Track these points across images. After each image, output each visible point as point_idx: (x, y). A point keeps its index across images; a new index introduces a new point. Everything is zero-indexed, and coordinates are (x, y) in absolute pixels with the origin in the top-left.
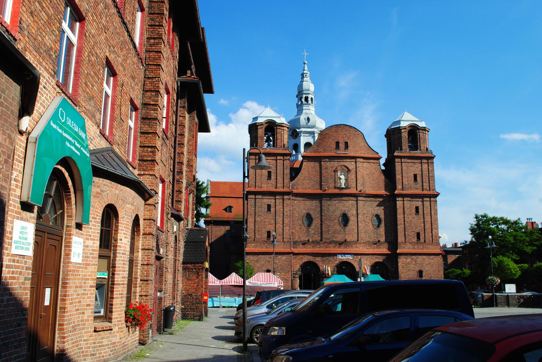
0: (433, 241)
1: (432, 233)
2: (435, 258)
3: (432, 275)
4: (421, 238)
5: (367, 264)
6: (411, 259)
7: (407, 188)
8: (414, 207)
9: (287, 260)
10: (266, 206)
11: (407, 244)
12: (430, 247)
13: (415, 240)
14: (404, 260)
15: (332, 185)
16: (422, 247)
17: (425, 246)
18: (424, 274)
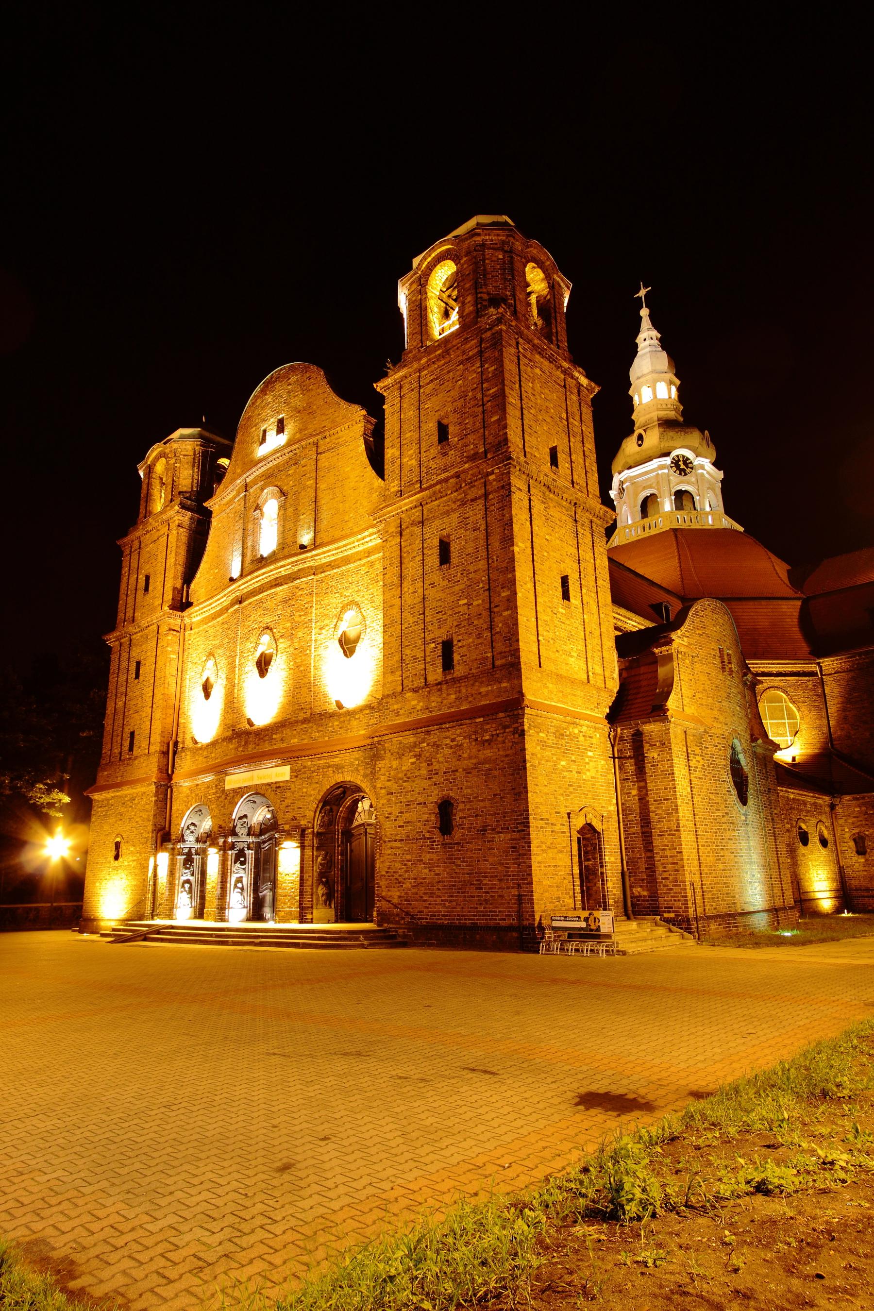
0: (498, 663)
1: (491, 628)
2: (499, 739)
3: (490, 820)
4: (456, 657)
5: (311, 795)
6: (415, 756)
7: (415, 480)
8: (436, 542)
9: (147, 806)
10: (135, 664)
11: (409, 695)
12: (483, 690)
13: (436, 674)
14: (395, 764)
15: (248, 559)
16: (453, 697)
17: (464, 691)
18: (458, 816)
